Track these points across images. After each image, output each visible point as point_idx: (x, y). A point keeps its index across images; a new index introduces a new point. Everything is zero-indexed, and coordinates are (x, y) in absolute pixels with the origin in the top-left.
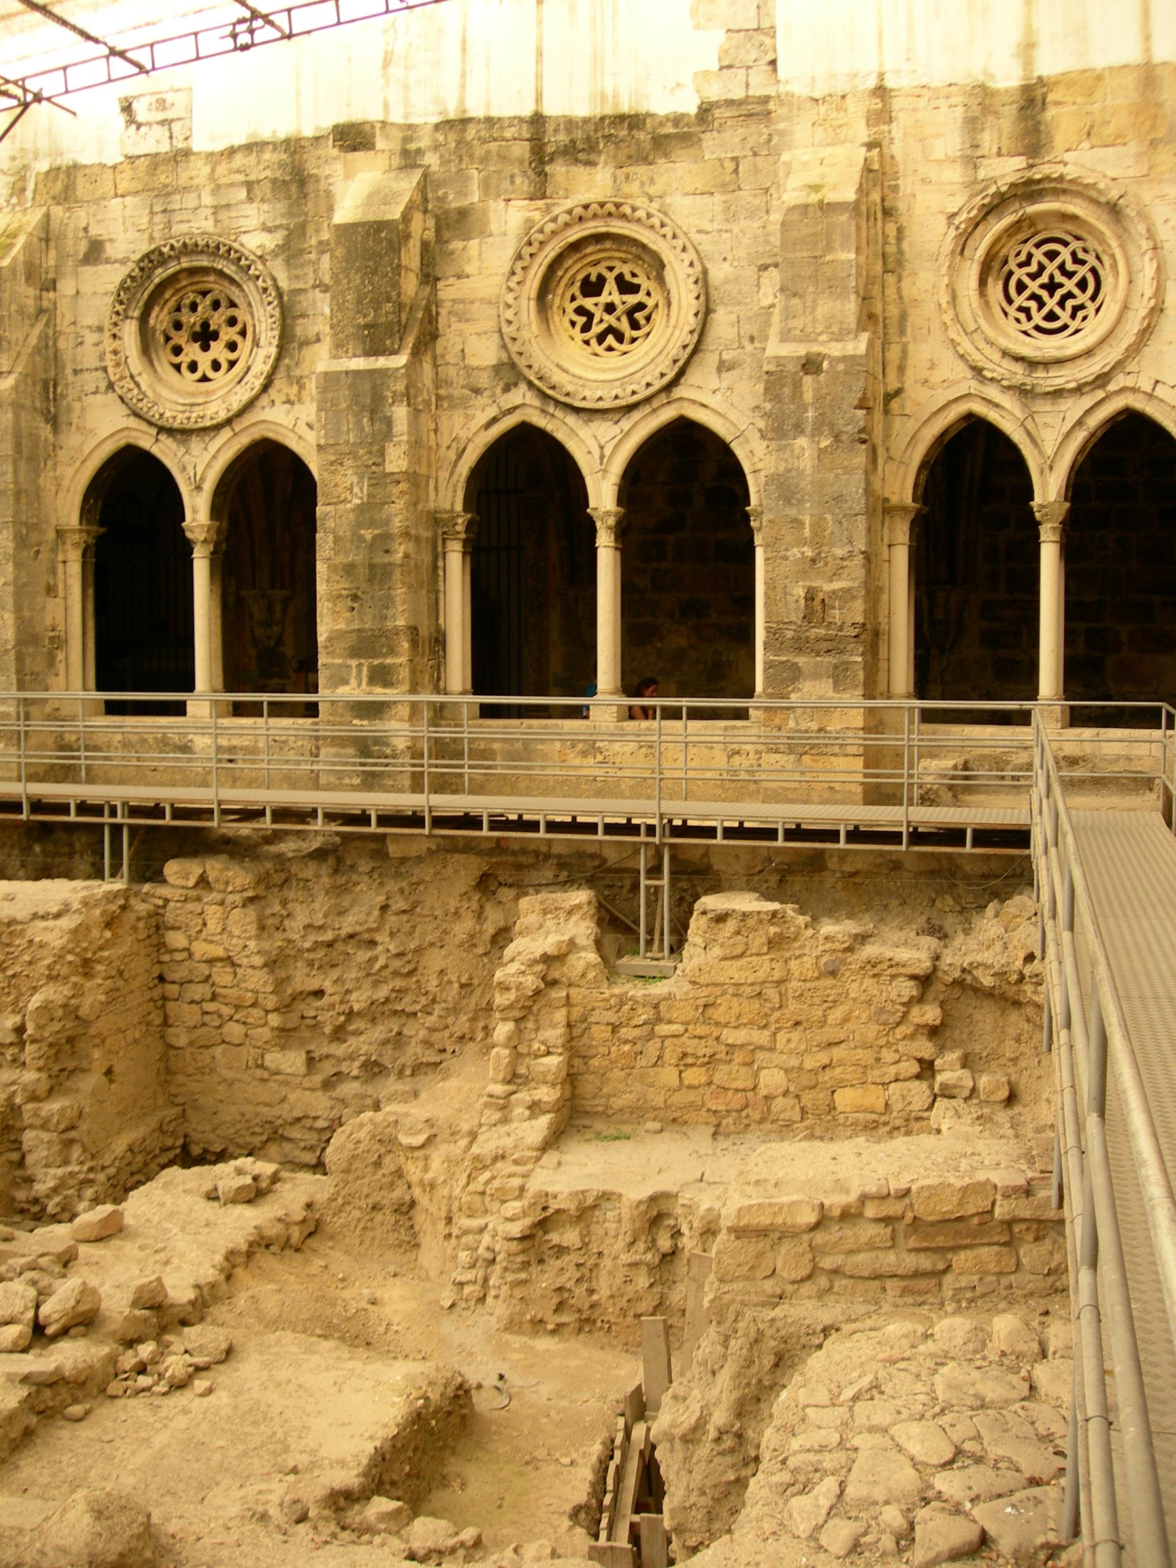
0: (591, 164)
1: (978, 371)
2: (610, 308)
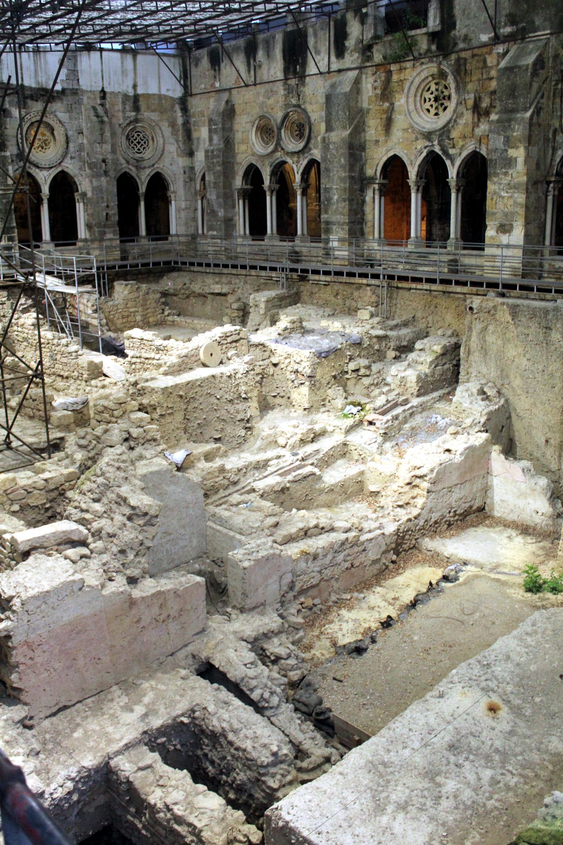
0: (37, 101)
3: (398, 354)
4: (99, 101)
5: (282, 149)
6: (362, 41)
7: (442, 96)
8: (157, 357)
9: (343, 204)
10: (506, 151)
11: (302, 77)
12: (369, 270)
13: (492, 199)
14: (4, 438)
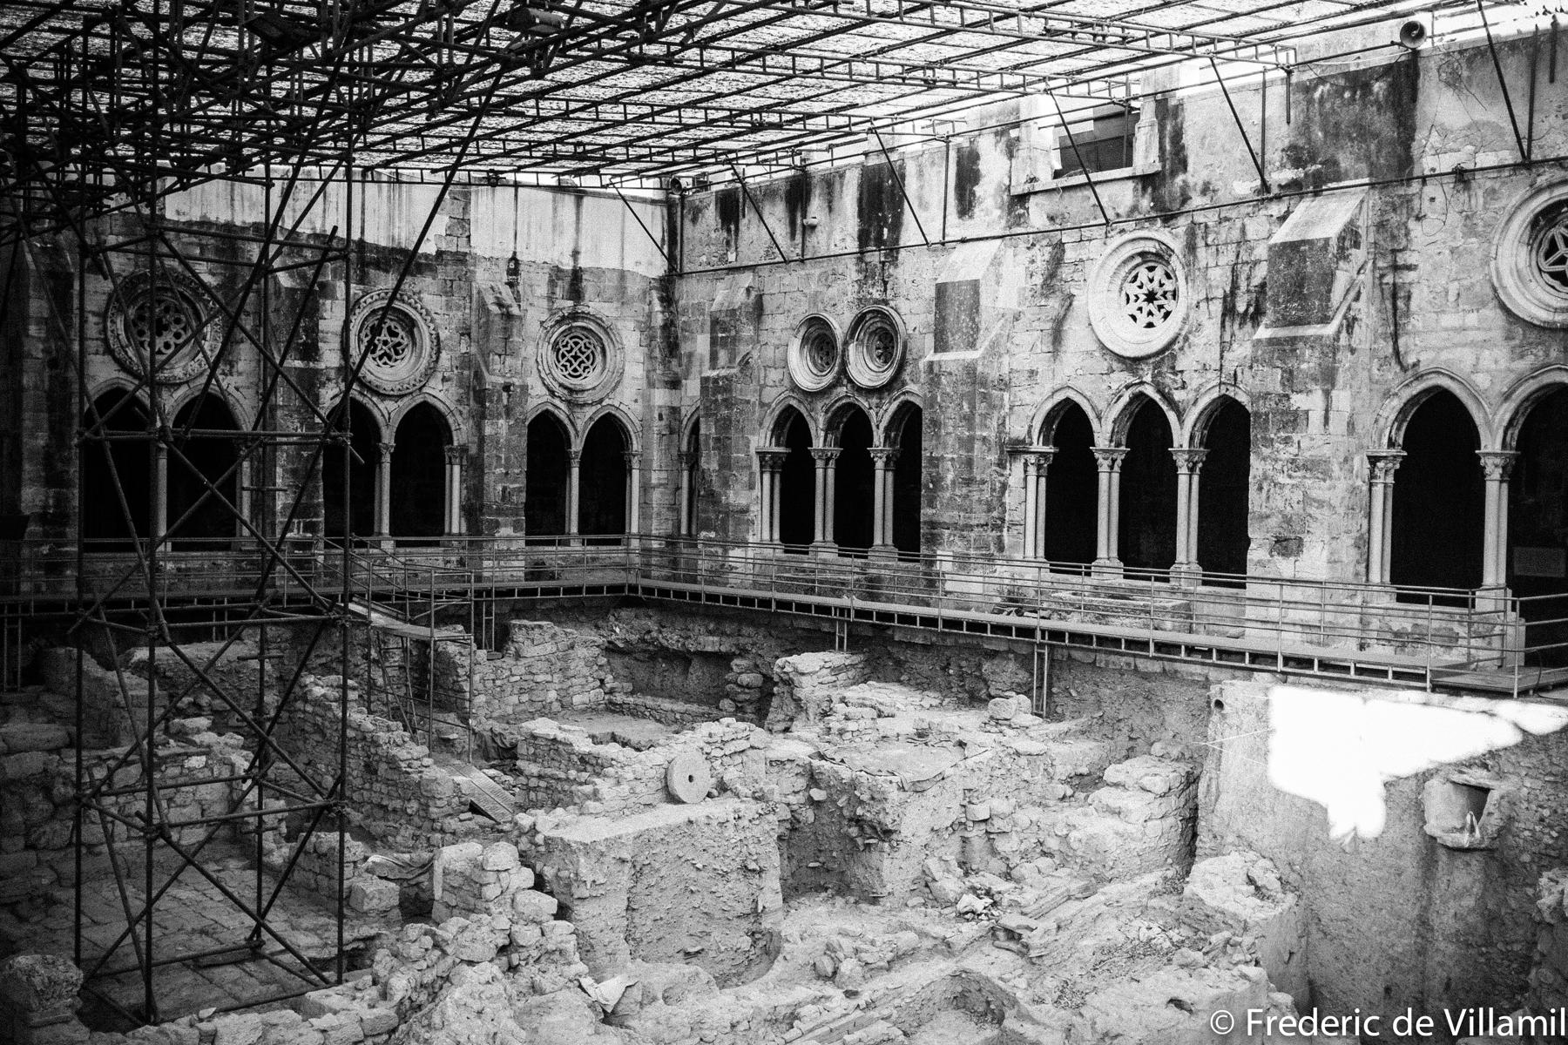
0: (387, 271)
1: (552, 393)
2: (385, 343)
3: (1069, 792)
4: (505, 278)
5: (850, 381)
6: (1008, 188)
7: (1160, 292)
8: (585, 775)
9: (965, 490)
10: (1288, 397)
11: (892, 250)
12: (1013, 620)
13: (1260, 488)
14: (248, 934)
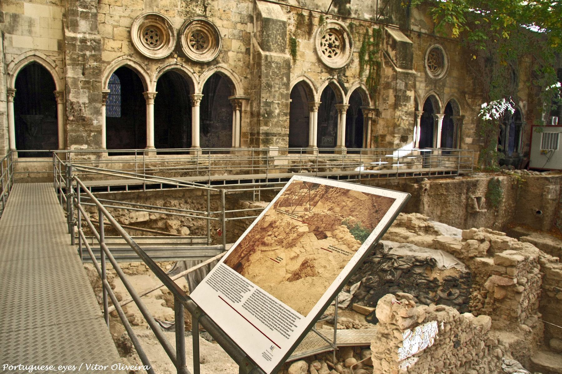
10: (406, 92)
